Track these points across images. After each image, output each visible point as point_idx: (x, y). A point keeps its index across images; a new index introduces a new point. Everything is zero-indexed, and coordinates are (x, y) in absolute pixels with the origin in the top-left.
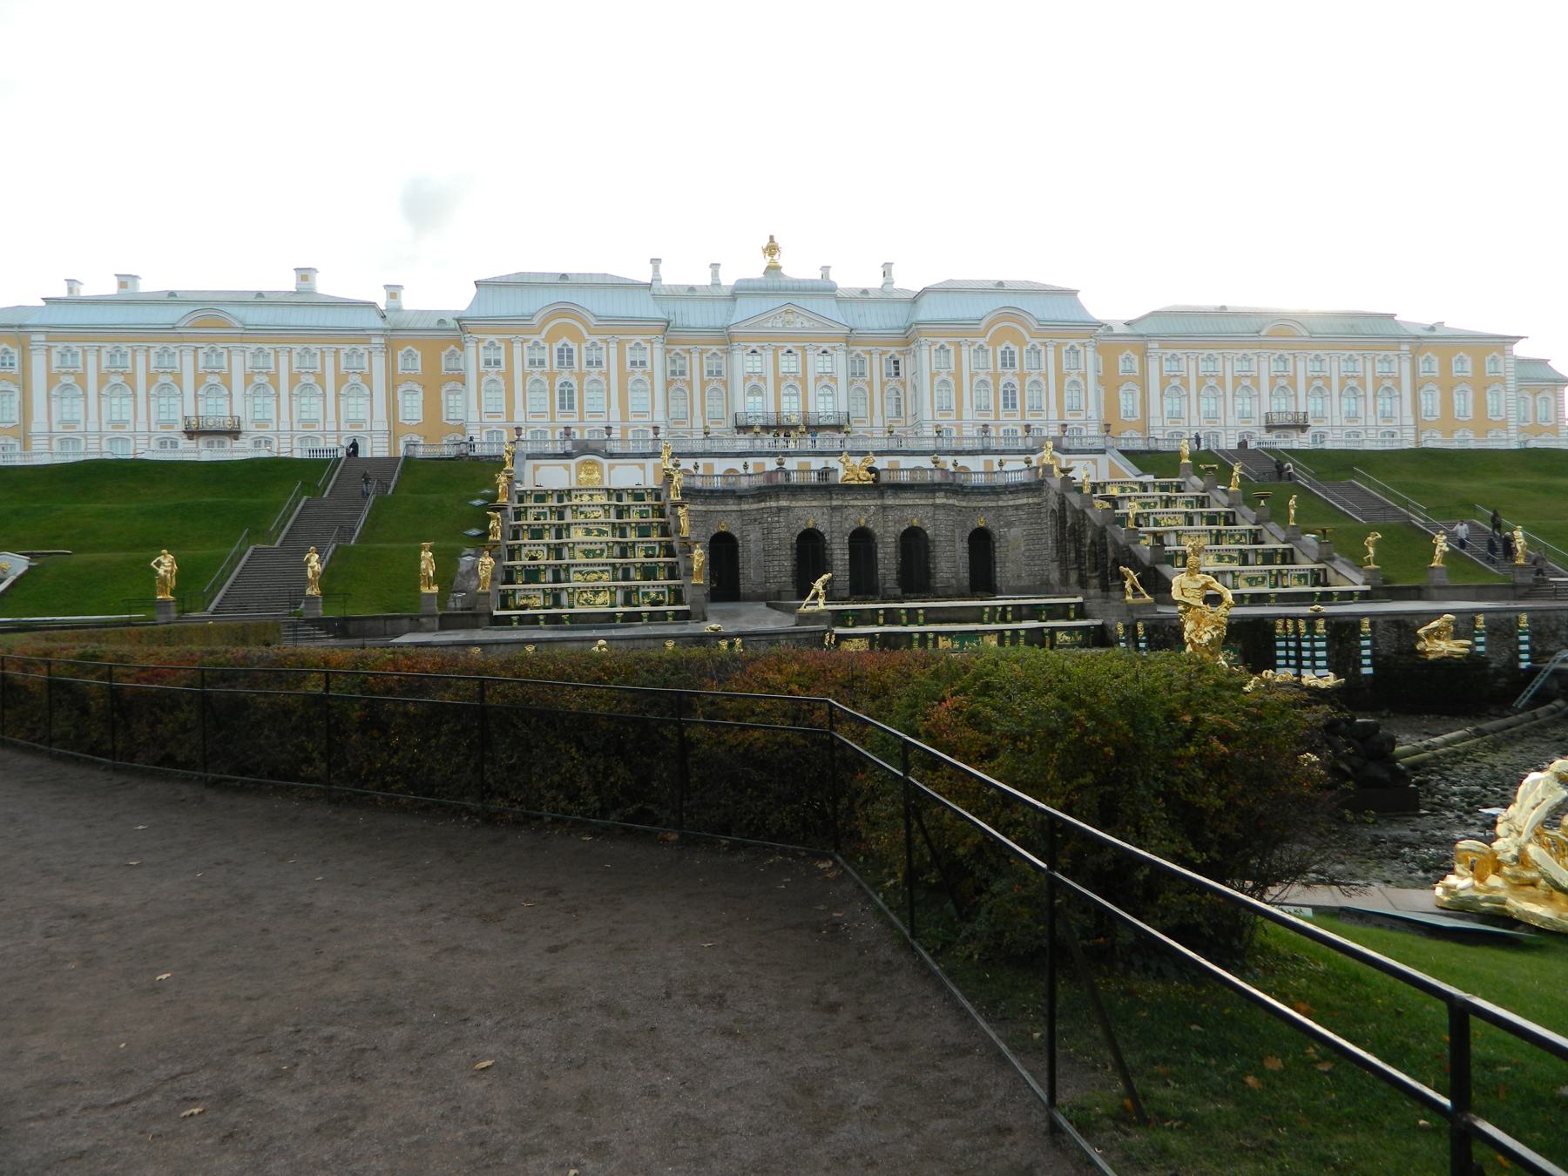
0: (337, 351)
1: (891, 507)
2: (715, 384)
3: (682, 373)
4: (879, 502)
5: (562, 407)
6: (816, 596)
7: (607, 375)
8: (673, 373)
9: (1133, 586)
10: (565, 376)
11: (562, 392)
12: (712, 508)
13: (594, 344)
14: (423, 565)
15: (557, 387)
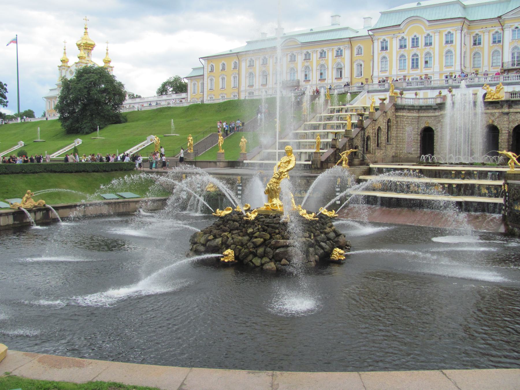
0: (333, 50)
1: (507, 114)
2: (496, 48)
3: (480, 44)
4: (500, 111)
5: (413, 67)
6: (342, 161)
7: (434, 48)
8: (475, 44)
9: (515, 164)
10: (415, 50)
11: (413, 60)
12: (422, 115)
13: (428, 35)
14: (219, 141)
15: (411, 57)
